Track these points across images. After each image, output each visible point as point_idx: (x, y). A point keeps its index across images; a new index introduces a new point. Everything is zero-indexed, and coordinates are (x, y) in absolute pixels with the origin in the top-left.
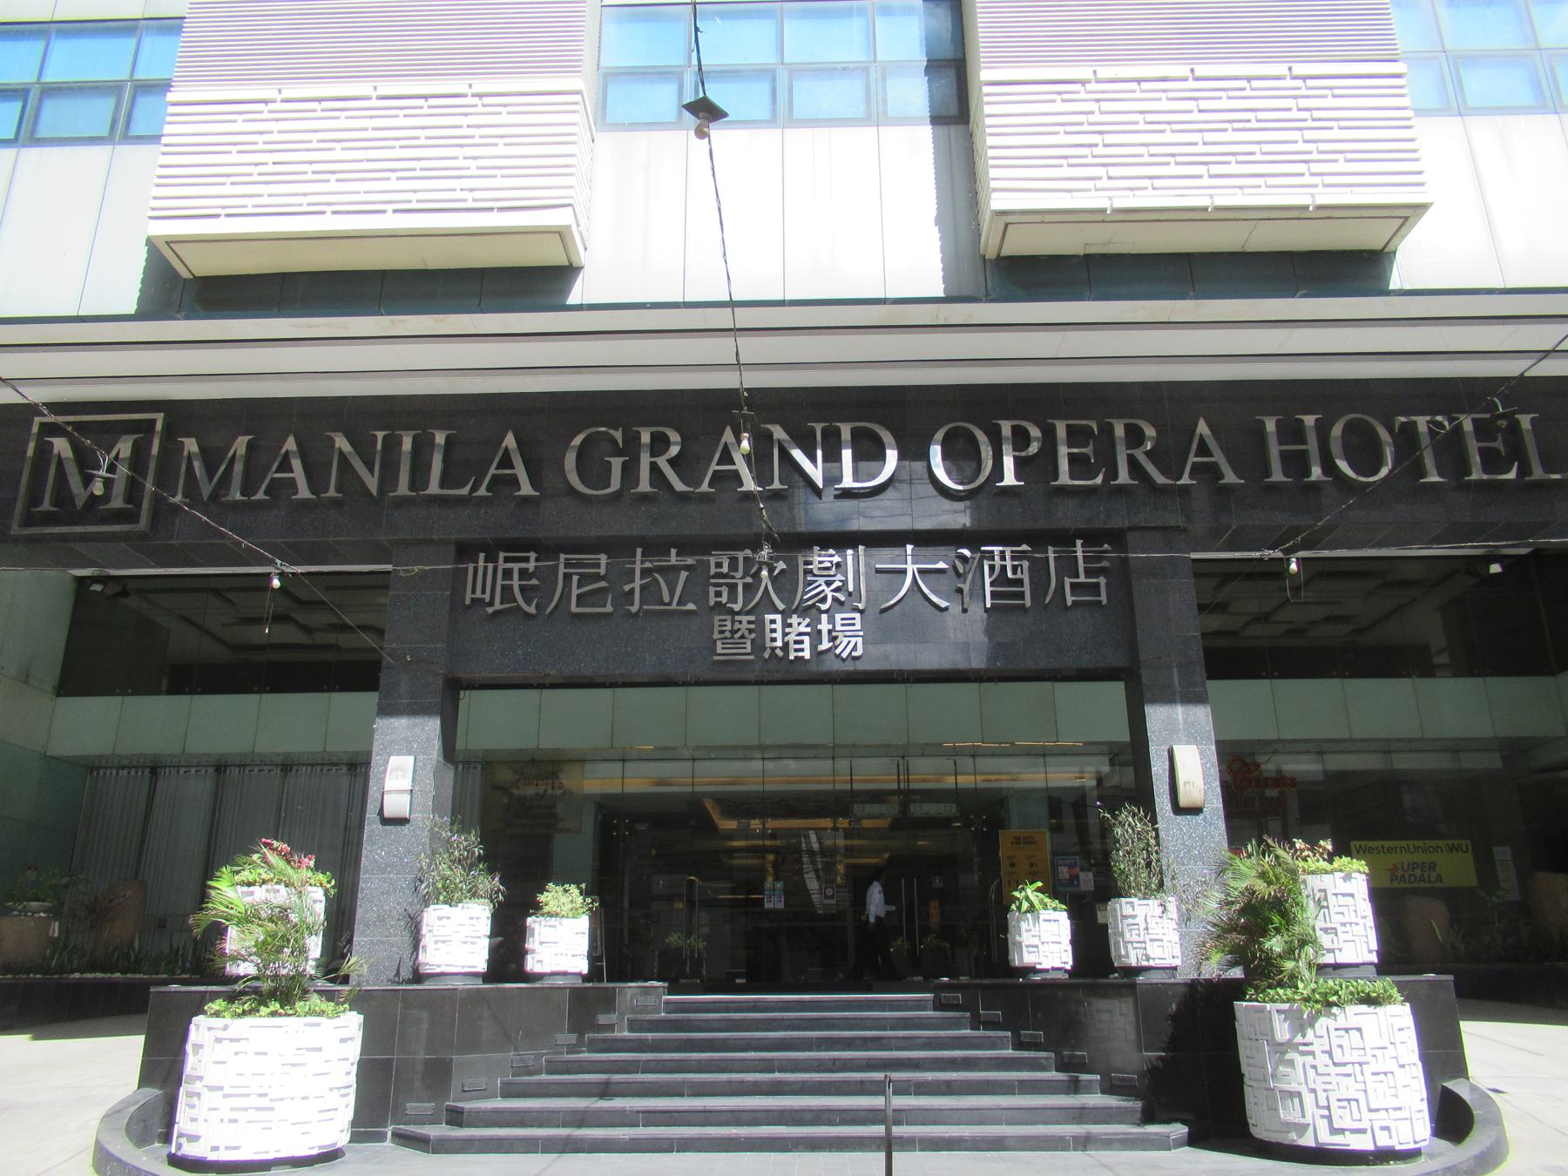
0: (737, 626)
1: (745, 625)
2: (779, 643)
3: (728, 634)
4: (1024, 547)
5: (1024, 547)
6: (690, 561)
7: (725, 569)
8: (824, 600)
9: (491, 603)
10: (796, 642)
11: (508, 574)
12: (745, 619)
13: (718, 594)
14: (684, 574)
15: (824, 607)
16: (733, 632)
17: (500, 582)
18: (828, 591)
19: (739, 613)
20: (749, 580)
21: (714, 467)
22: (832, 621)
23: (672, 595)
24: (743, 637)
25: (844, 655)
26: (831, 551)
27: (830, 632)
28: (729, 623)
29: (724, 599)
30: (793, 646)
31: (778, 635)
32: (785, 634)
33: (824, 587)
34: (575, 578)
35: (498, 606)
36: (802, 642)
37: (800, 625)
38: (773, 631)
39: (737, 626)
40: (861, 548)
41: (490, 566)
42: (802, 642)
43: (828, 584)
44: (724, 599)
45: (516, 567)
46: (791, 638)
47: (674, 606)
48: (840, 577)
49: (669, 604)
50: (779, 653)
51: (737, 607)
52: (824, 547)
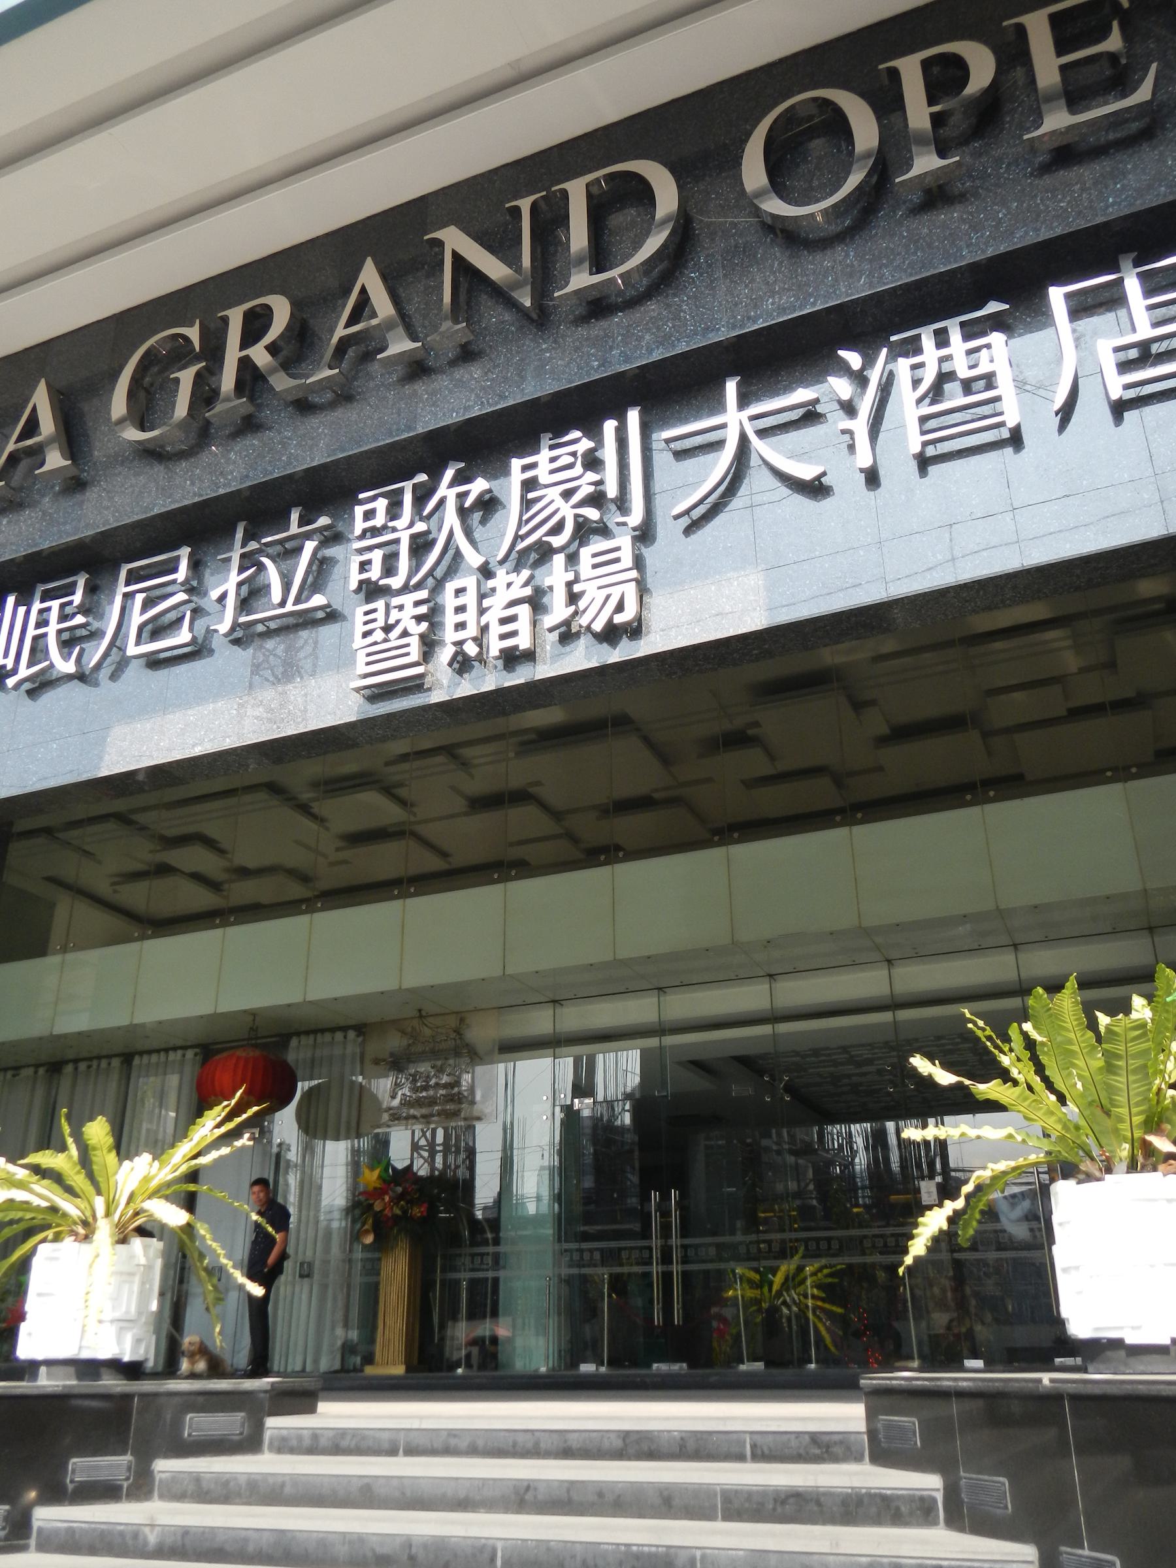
0: (395, 615)
1: (410, 611)
2: (472, 631)
3: (379, 635)
4: (993, 307)
5: (993, 307)
6: (323, 521)
7: (379, 520)
8: (557, 529)
9: (14, 671)
10: (504, 621)
11: (42, 623)
12: (408, 599)
13: (364, 566)
14: (310, 546)
15: (557, 541)
16: (387, 629)
17: (31, 632)
18: (567, 512)
19: (406, 589)
20: (420, 527)
21: (340, 332)
22: (572, 559)
23: (287, 587)
24: (405, 634)
25: (598, 626)
26: (576, 434)
27: (569, 585)
28: (380, 615)
29: (375, 573)
30: (496, 630)
31: (470, 617)
32: (482, 611)
33: (559, 502)
34: (140, 598)
35: (24, 672)
36: (512, 619)
37: (509, 585)
38: (461, 609)
39: (395, 615)
40: (633, 416)
41: (22, 610)
42: (512, 619)
43: (567, 495)
44: (375, 573)
45: (55, 604)
46: (491, 618)
47: (289, 607)
48: (591, 476)
49: (283, 604)
50: (471, 649)
51: (396, 582)
52: (559, 429)
